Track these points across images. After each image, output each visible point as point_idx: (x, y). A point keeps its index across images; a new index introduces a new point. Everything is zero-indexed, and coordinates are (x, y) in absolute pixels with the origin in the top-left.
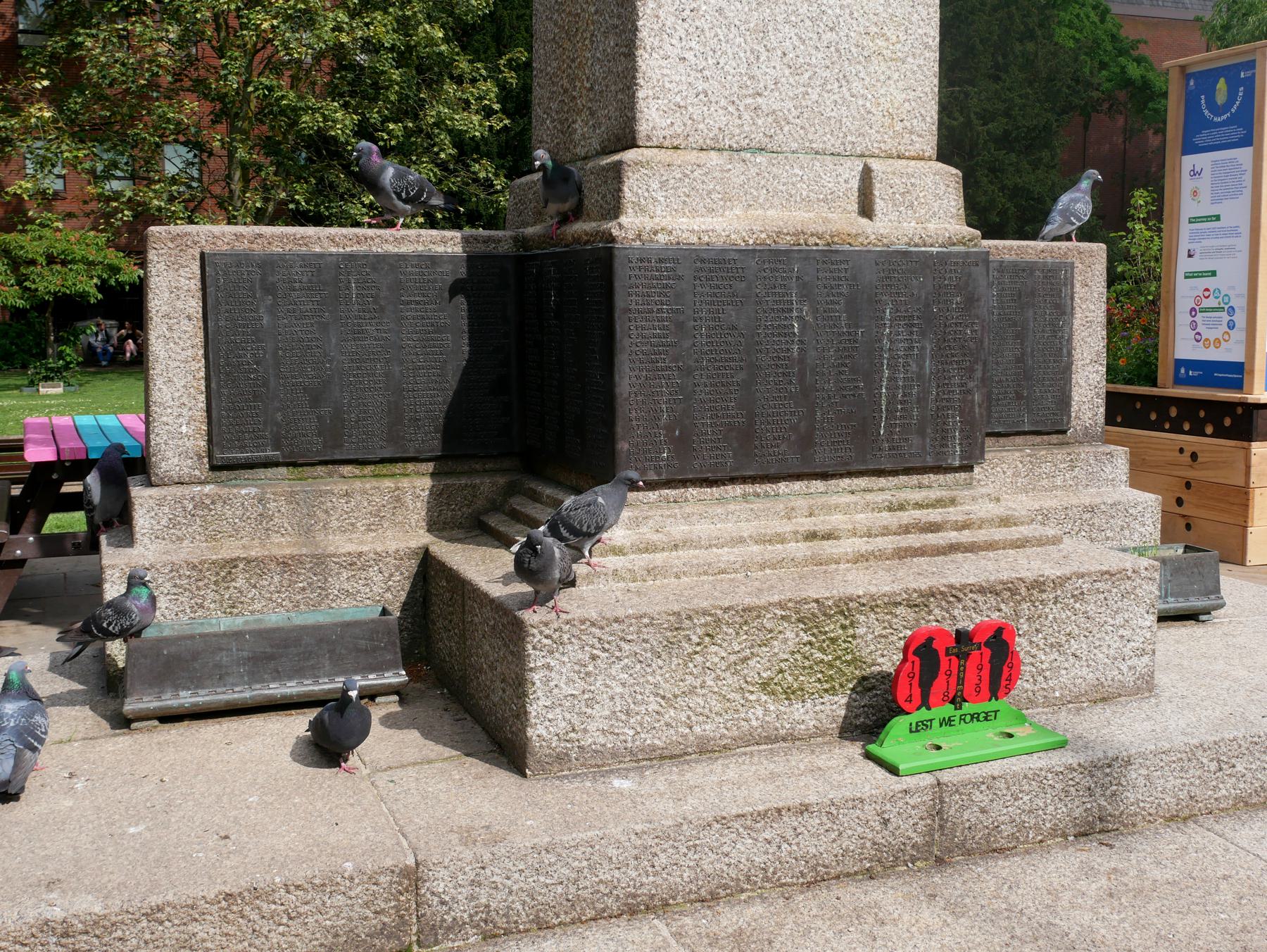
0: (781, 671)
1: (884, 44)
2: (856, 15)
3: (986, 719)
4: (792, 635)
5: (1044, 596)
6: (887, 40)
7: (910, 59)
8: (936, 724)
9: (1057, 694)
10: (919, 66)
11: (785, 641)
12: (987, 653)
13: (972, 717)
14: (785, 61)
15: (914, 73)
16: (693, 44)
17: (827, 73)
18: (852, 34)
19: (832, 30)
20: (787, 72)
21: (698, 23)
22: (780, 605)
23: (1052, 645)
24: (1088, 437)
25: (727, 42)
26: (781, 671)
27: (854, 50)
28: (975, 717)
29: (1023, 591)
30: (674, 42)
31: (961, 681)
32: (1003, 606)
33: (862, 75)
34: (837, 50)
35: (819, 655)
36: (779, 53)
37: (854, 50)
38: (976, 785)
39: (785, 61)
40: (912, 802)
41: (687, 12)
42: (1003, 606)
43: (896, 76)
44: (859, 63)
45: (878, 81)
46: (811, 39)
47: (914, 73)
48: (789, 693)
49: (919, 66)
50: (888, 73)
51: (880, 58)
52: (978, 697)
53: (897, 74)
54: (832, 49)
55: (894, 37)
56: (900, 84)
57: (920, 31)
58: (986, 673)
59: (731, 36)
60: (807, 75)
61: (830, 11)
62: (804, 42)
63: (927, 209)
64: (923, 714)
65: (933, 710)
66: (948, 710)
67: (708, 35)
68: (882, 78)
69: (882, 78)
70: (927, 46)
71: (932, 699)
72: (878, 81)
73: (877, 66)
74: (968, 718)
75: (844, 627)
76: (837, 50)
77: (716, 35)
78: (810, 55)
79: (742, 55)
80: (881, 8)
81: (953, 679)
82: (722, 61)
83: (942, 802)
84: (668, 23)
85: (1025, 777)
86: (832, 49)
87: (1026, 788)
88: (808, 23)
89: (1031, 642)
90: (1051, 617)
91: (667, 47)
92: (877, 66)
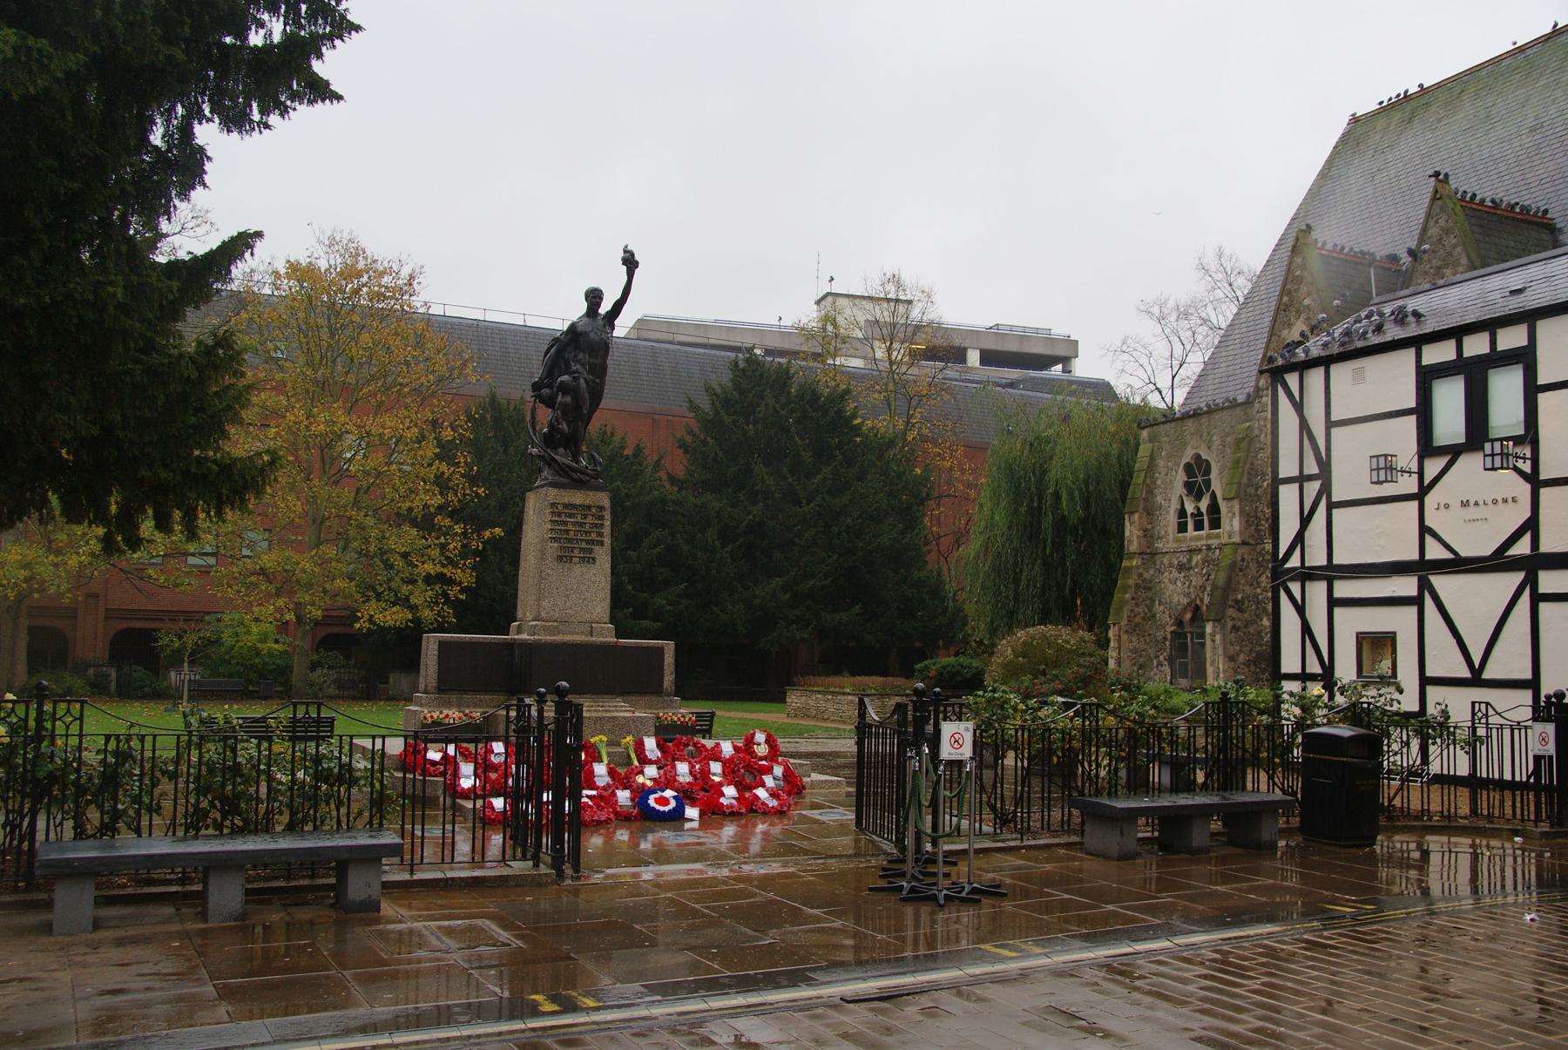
24: (669, 695)
63: (606, 635)
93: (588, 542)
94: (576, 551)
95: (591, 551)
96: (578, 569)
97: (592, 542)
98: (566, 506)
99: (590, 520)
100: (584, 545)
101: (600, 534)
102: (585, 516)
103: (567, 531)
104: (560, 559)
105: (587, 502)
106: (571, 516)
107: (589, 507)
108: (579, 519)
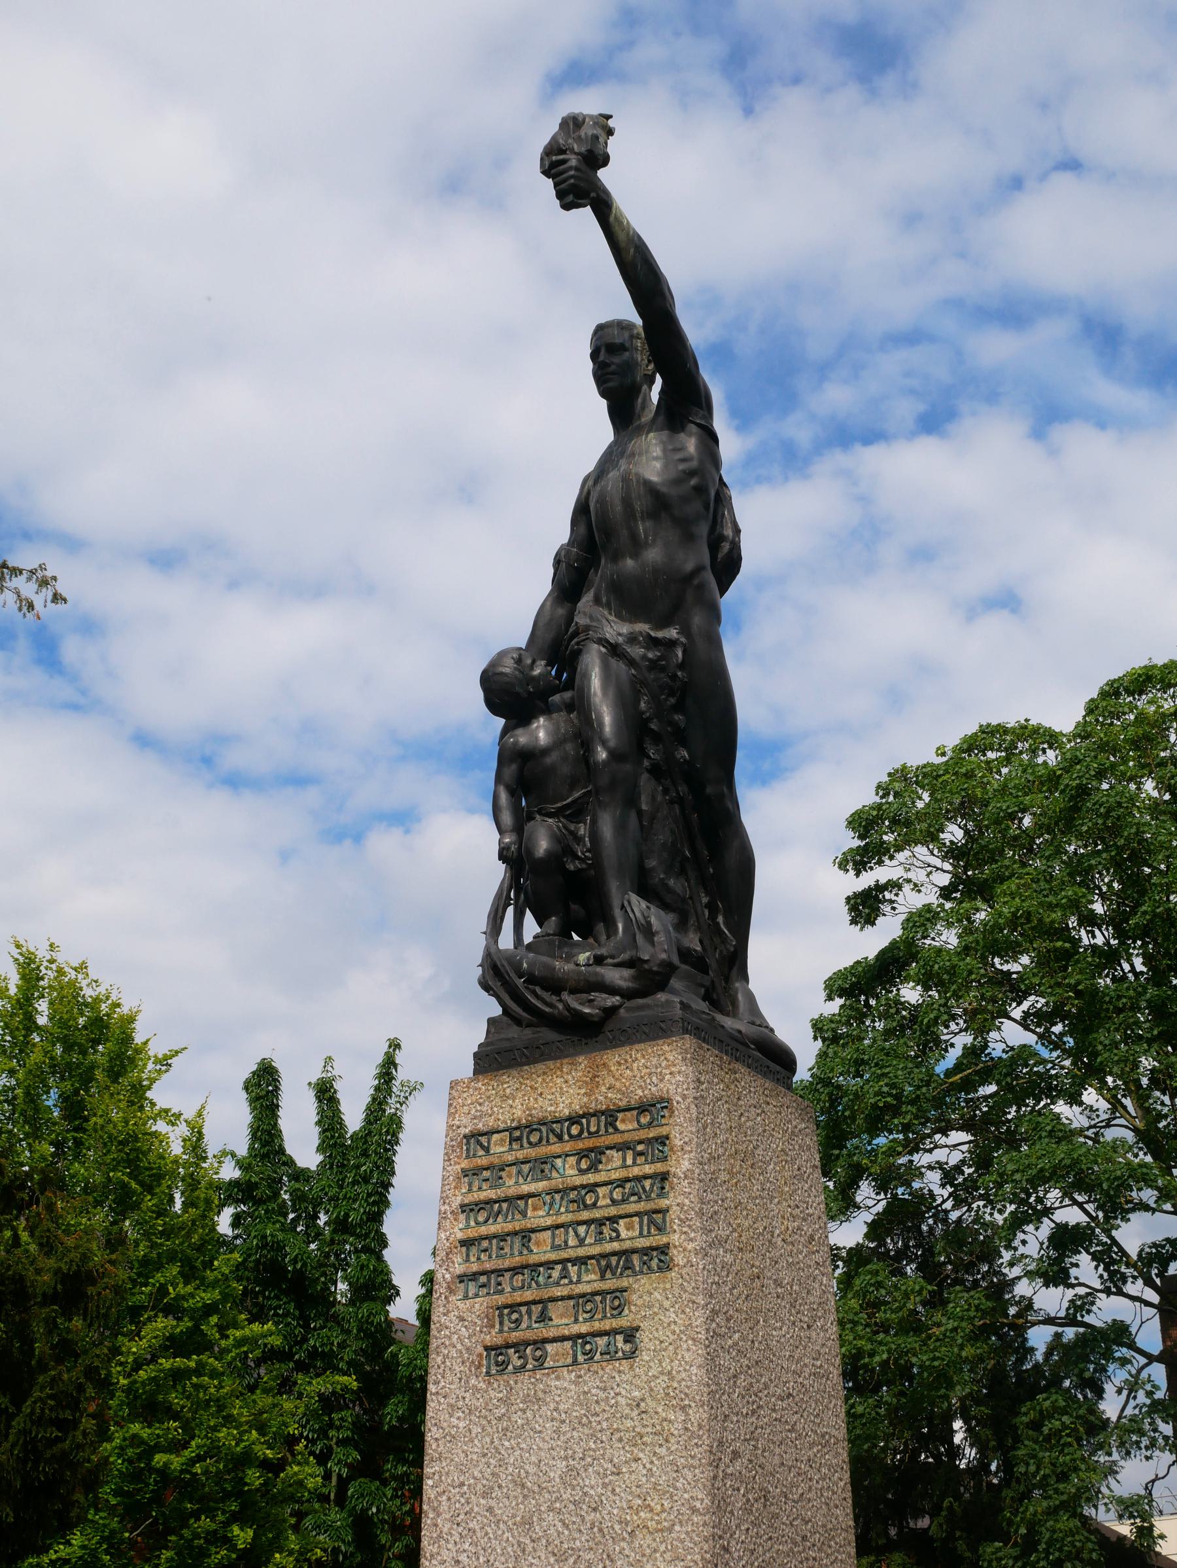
1: (649, 1515)
2: (618, 1490)
6: (652, 1511)
7: (677, 1528)
10: (687, 1533)
14: (550, 1549)
15: (682, 1541)
16: (466, 1546)
17: (590, 1556)
18: (615, 1512)
19: (595, 1510)
20: (552, 1560)
21: (471, 1525)
25: (496, 1538)
27: (617, 1527)
30: (450, 1546)
33: (627, 1552)
34: (601, 1530)
36: (544, 1541)
37: (617, 1527)
39: (550, 1549)
41: (462, 1517)
43: (662, 1548)
44: (624, 1539)
45: (643, 1555)
46: (574, 1523)
47: (682, 1541)
49: (687, 1533)
50: (654, 1545)
51: (645, 1531)
53: (664, 1545)
54: (596, 1529)
55: (659, 1507)
56: (668, 1556)
57: (686, 1496)
59: (500, 1532)
60: (571, 1560)
61: (592, 1492)
62: (567, 1527)
67: (479, 1535)
68: (648, 1551)
69: (648, 1551)
70: (694, 1510)
72: (643, 1555)
73: (644, 1541)
76: (601, 1530)
77: (487, 1534)
78: (574, 1539)
79: (510, 1549)
80: (644, 1479)
82: (492, 1558)
84: (445, 1530)
86: (596, 1529)
88: (572, 1507)
91: (445, 1553)
92: (644, 1541)
93: (606, 1264)
94: (562, 1321)
95: (617, 1299)
96: (563, 1386)
97: (622, 1261)
98: (519, 1133)
99: (614, 1166)
100: (590, 1281)
101: (656, 1219)
102: (593, 1157)
103: (526, 1235)
104: (498, 1358)
105: (603, 1098)
106: (541, 1167)
107: (610, 1116)
108: (569, 1172)
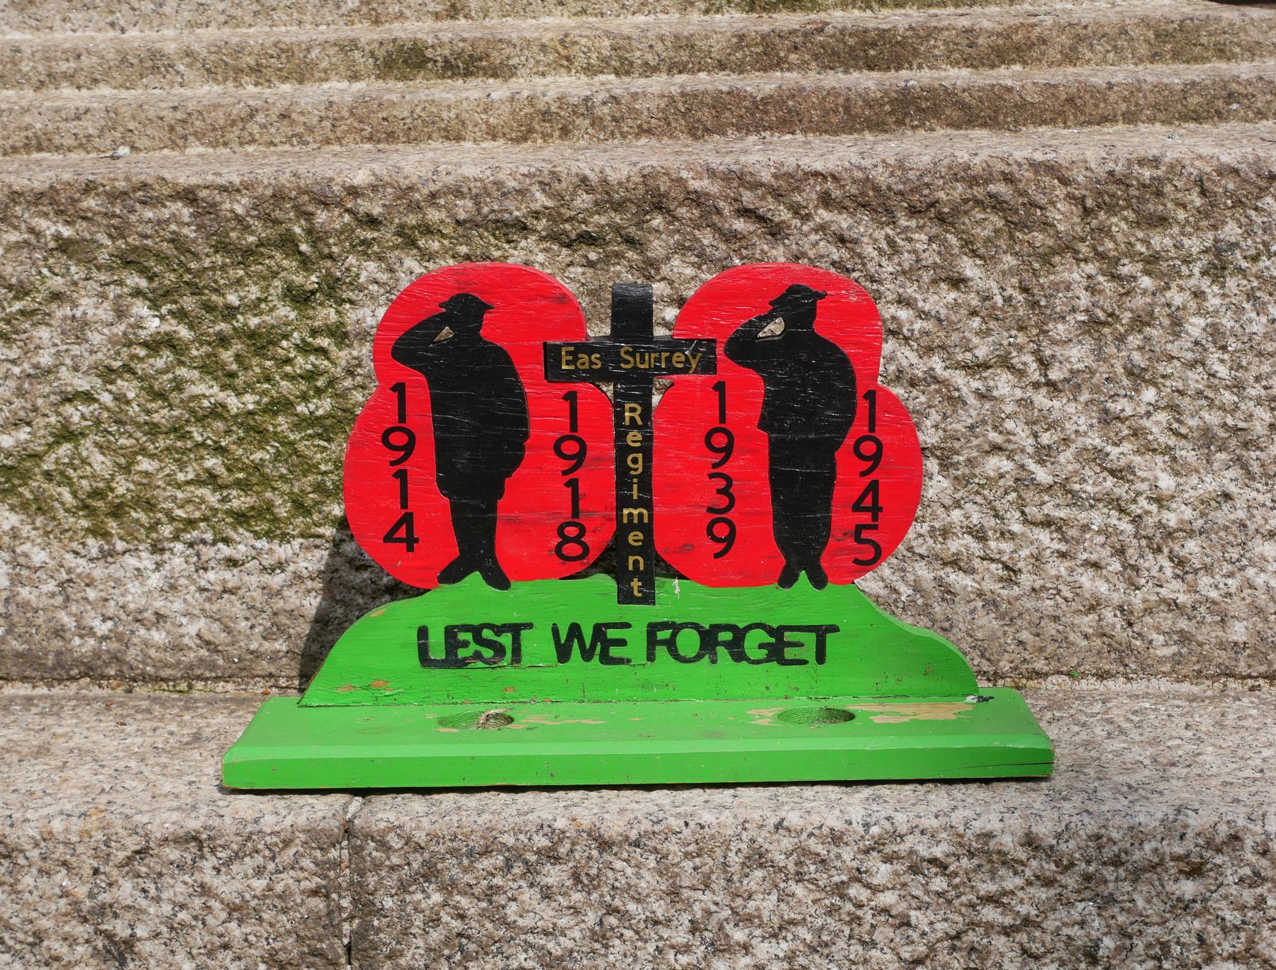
0: (66, 434)
3: (776, 652)
4: (104, 313)
5: (1160, 241)
8: (538, 645)
9: (1238, 631)
11: (79, 329)
12: (751, 389)
13: (709, 639)
22: (47, 199)
23: (1206, 439)
26: (66, 434)
28: (718, 640)
29: (1063, 216)
31: (632, 485)
32: (969, 267)
35: (206, 390)
38: (525, 862)
40: (227, 887)
42: (969, 267)
48: (103, 512)
52: (722, 558)
58: (751, 469)
64: (471, 600)
65: (521, 589)
66: (593, 599)
71: (507, 546)
74: (689, 642)
75: (299, 298)
81: (598, 476)
83: (365, 907)
85: (757, 858)
87: (766, 905)
89: (1107, 418)
90: (1195, 326)
